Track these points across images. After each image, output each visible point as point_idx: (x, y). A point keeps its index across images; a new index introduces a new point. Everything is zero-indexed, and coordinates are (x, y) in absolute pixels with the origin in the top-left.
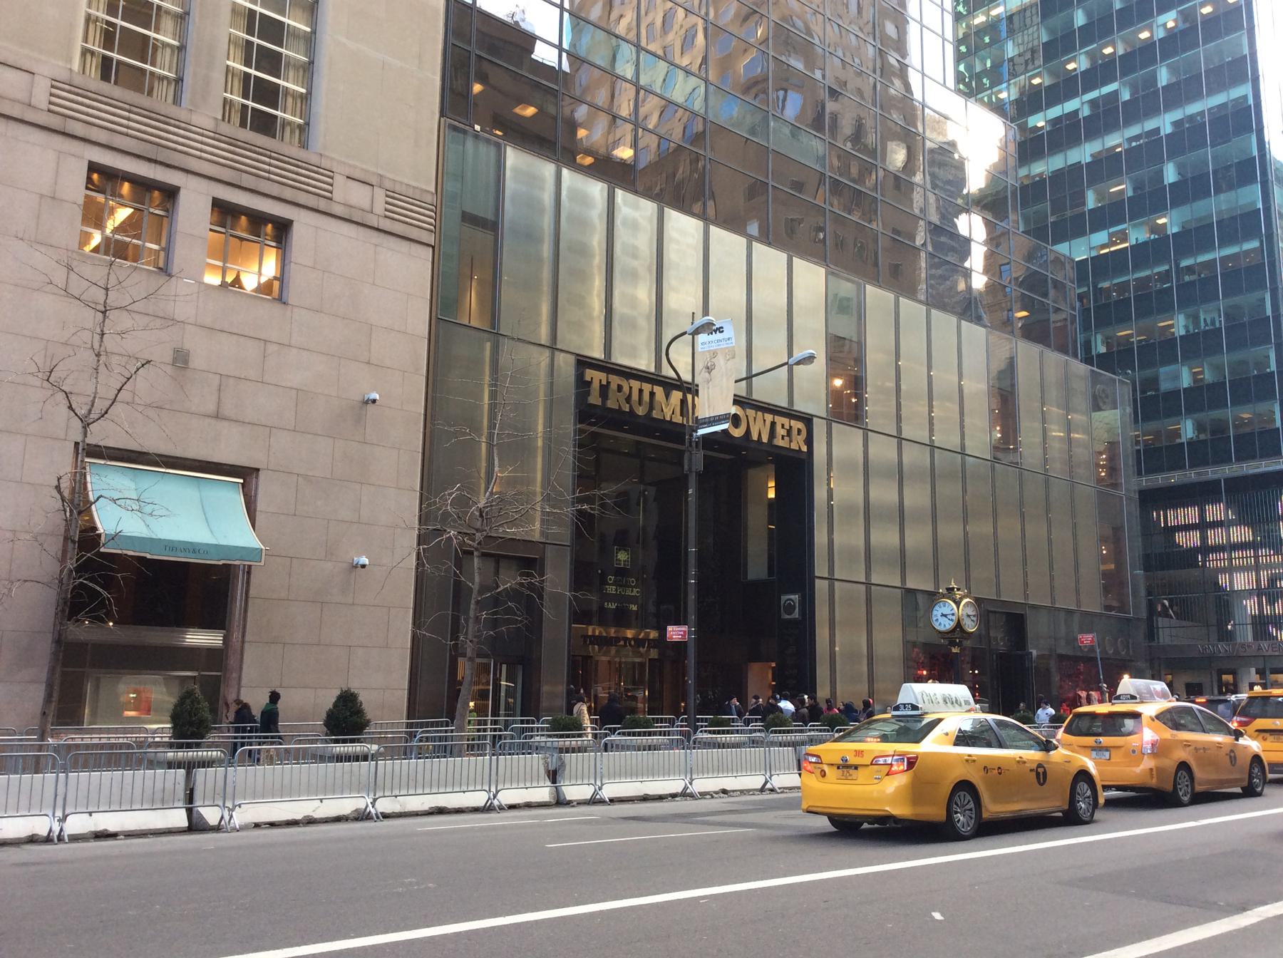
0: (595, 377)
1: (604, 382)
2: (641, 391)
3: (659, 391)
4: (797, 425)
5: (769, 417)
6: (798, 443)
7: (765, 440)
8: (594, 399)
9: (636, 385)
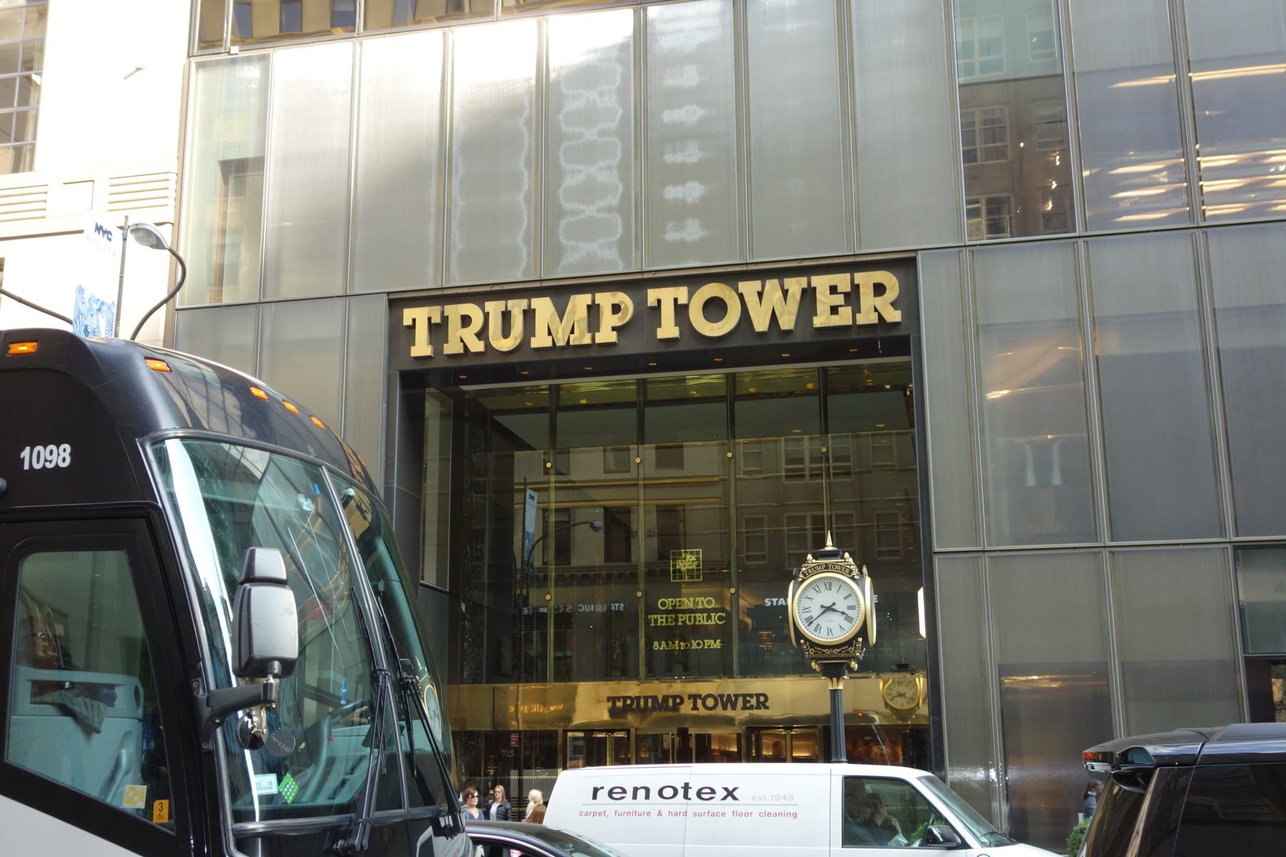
0: (418, 316)
1: (436, 319)
2: (506, 315)
3: (543, 306)
4: (866, 280)
5: (795, 285)
6: (878, 308)
7: (787, 322)
8: (422, 347)
9: (491, 306)
